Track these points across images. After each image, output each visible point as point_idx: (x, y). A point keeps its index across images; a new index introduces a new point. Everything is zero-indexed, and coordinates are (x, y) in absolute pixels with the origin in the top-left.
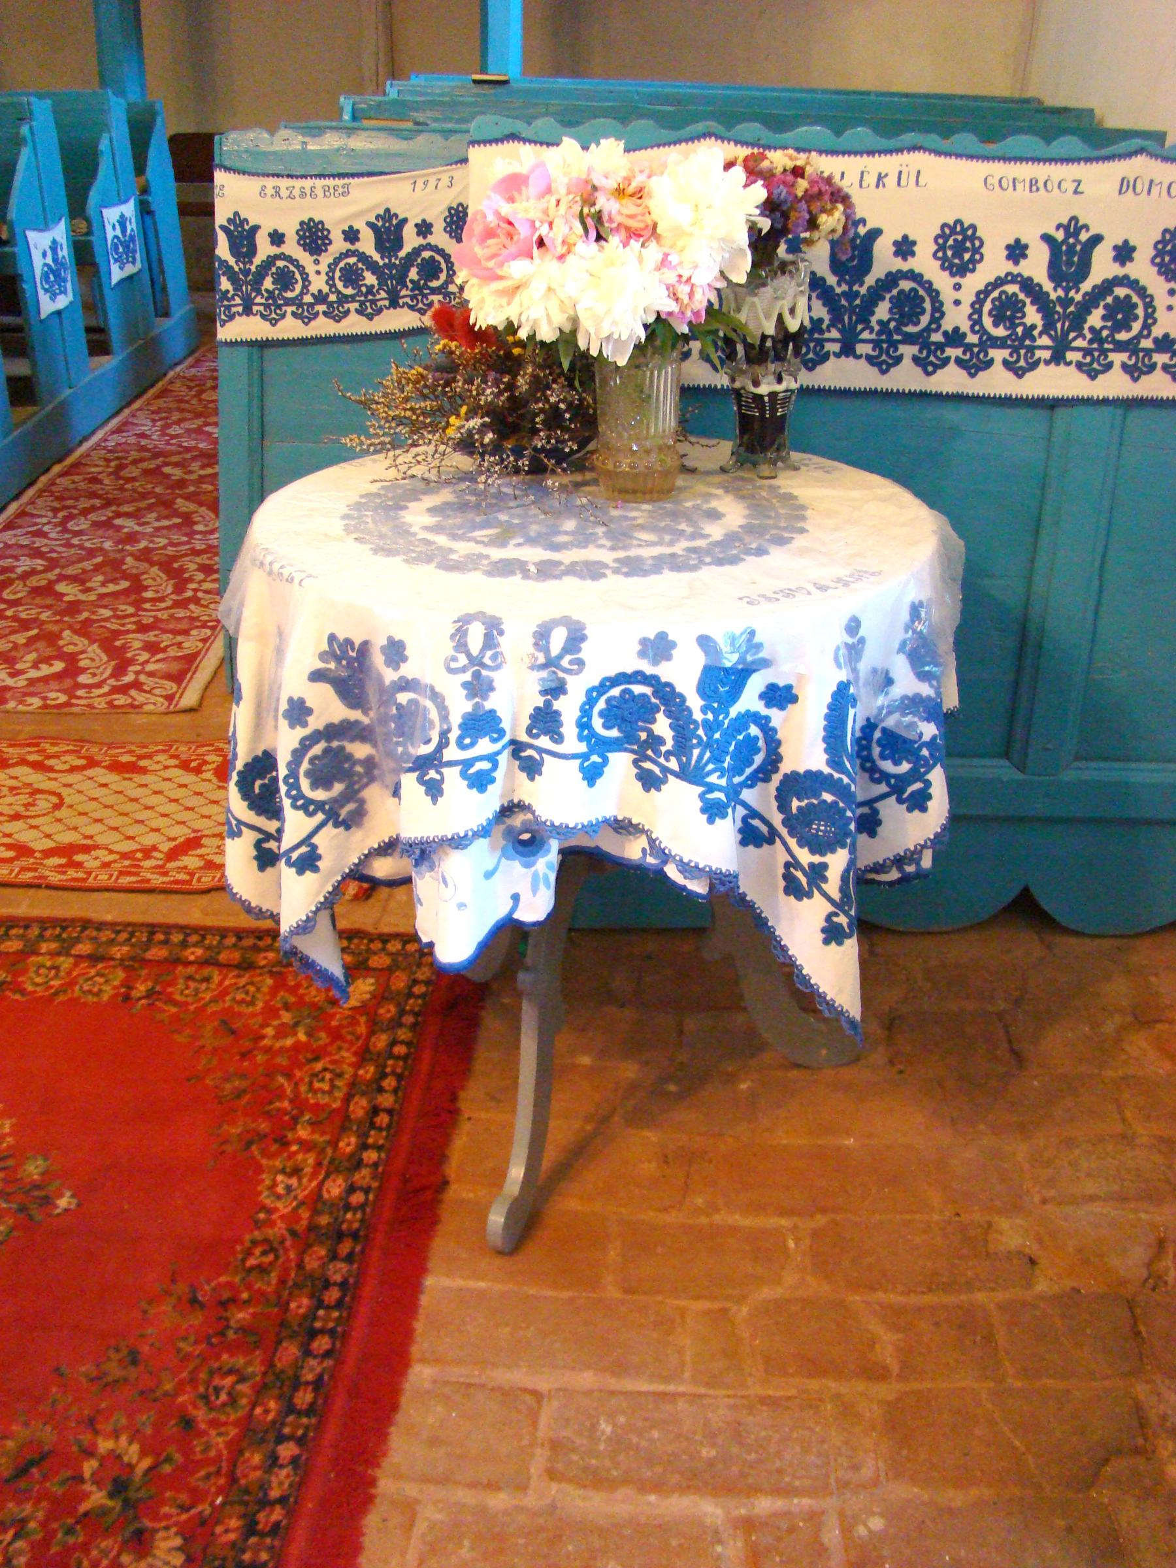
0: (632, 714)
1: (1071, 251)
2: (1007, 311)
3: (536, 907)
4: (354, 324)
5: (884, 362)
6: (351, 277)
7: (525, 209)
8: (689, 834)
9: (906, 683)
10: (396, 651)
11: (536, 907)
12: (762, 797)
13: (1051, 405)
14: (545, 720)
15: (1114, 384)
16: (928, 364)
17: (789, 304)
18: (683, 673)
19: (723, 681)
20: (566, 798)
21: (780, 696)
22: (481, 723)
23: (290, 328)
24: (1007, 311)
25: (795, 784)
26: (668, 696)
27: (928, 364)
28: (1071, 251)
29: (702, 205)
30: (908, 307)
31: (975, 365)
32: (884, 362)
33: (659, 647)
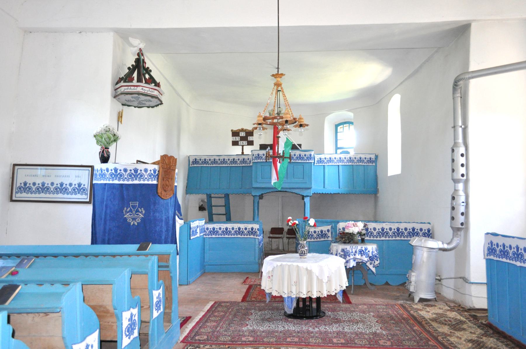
0: (361, 252)
1: (383, 229)
2: (379, 233)
3: (355, 265)
4: (318, 240)
5: (370, 237)
6: (318, 235)
7: (350, 225)
8: (365, 259)
9: (376, 252)
10: (346, 249)
11: (355, 265)
12: (368, 258)
13: (383, 240)
14: (356, 252)
15: (387, 239)
16: (373, 237)
17: (364, 232)
18: (363, 249)
19: (366, 249)
20: (358, 256)
21: (369, 251)
22: (352, 252)
23: (313, 240)
24: (379, 233)
25: (370, 257)
26: (363, 250)
27: (373, 237)
28: (383, 229)
29: (360, 226)
30: (371, 233)
31: (377, 237)
32: (370, 237)
33: (362, 248)
